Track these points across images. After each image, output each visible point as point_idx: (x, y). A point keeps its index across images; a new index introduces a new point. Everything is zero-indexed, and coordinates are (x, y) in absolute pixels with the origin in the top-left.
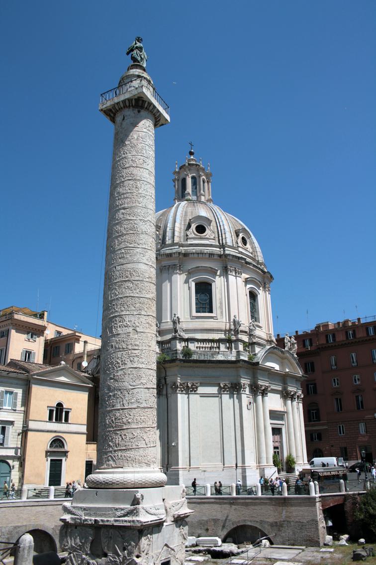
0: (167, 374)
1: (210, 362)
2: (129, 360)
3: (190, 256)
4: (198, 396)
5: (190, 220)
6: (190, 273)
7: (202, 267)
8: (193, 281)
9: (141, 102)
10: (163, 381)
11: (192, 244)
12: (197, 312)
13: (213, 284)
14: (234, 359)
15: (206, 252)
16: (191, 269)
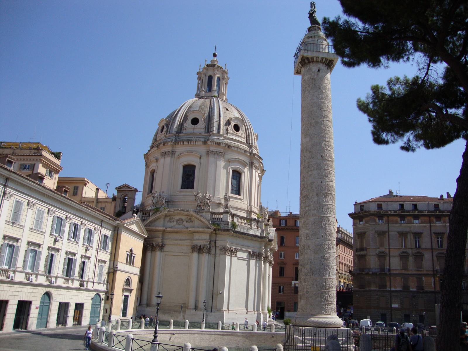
0: (217, 239)
1: (244, 234)
2: (332, 247)
3: (232, 149)
4: (236, 258)
5: (232, 118)
6: (229, 161)
7: (239, 159)
8: (231, 168)
9: (331, 63)
10: (213, 244)
11: (232, 139)
12: (231, 193)
13: (243, 174)
14: (259, 235)
15: (241, 148)
16: (232, 159)
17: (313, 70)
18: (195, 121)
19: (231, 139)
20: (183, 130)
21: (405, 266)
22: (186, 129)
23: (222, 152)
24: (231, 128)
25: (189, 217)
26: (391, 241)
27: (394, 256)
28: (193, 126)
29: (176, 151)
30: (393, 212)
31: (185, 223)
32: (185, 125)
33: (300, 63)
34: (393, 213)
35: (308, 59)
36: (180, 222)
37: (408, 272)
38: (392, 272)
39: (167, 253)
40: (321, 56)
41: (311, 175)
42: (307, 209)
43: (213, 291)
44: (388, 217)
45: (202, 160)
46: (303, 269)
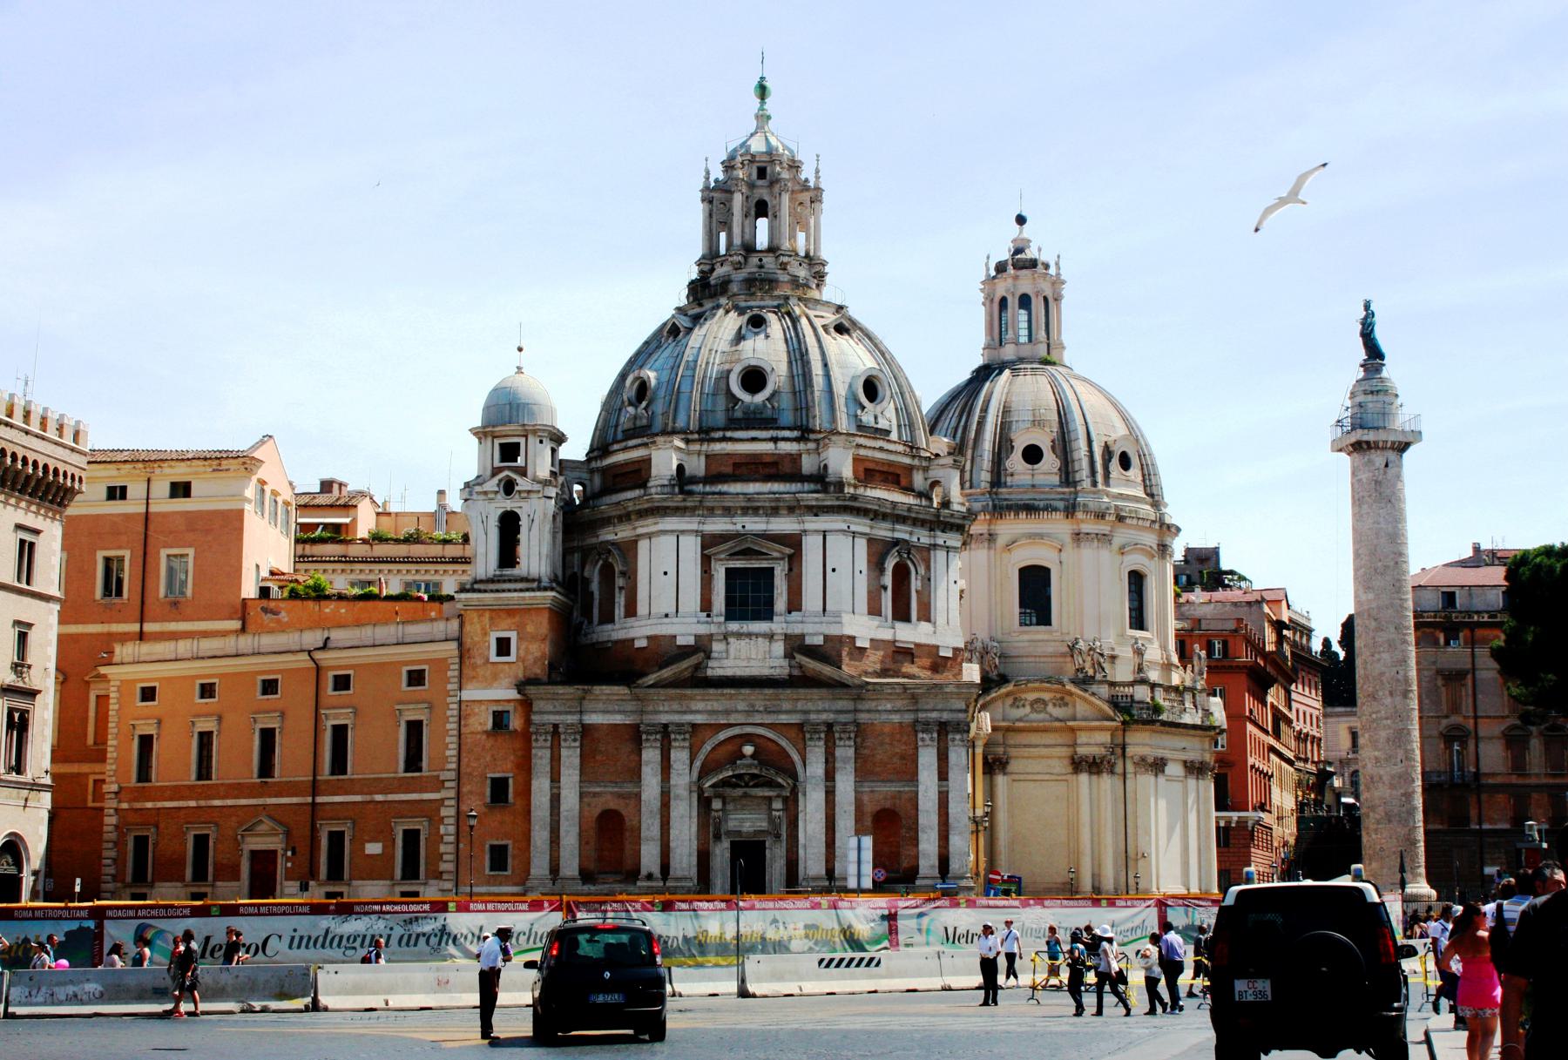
0: (1128, 740)
10: (1119, 751)
12: (1131, 628)
14: (1199, 723)
17: (1377, 464)
18: (1033, 455)
19: (1121, 496)
20: (1006, 476)
21: (1518, 765)
22: (1012, 475)
23: (1107, 533)
24: (1115, 465)
25: (1058, 696)
26: (1480, 696)
27: (1491, 738)
28: (1029, 466)
29: (998, 532)
30: (1486, 616)
31: (1050, 708)
32: (1008, 464)
33: (1352, 445)
34: (1486, 619)
35: (1368, 443)
36: (1039, 706)
37: (1528, 781)
38: (1483, 781)
39: (1016, 777)
40: (1392, 438)
41: (1379, 660)
42: (1374, 716)
43: (1126, 852)
44: (1472, 631)
45: (1063, 554)
46: (1371, 814)
